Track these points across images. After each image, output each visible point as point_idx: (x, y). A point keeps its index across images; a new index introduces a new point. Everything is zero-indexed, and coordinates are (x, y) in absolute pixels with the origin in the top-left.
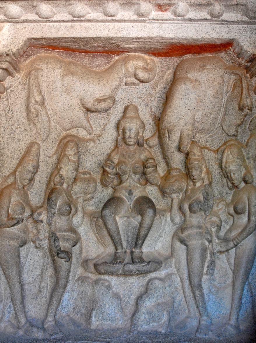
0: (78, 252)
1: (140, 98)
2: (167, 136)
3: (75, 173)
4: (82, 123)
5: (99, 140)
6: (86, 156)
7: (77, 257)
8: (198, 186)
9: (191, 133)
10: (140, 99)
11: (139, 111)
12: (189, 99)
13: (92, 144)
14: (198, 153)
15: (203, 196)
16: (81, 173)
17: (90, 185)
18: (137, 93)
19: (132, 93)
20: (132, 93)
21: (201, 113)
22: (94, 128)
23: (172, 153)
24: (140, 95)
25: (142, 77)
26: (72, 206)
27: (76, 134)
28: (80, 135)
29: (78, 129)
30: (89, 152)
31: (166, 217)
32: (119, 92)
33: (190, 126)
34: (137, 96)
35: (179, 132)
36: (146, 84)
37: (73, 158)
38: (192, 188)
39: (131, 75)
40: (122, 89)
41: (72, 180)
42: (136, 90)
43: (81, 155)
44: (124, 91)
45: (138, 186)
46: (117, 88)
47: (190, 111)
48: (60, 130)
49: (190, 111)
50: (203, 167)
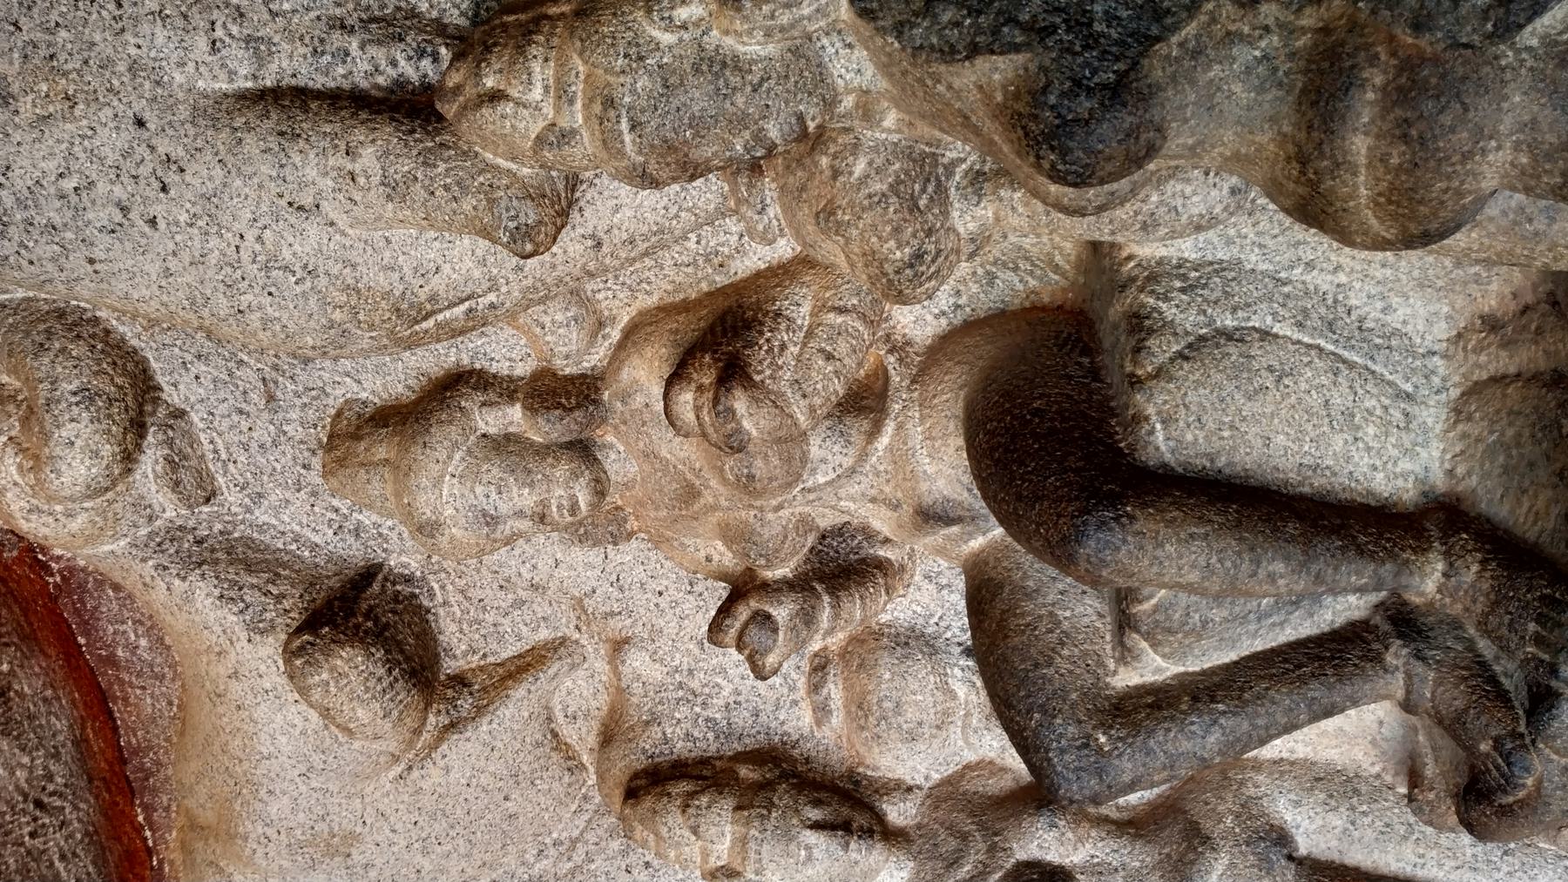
0: (1338, 821)
1: (271, 398)
2: (459, 310)
3: (811, 837)
4: (516, 727)
5: (612, 614)
6: (718, 685)
7: (1370, 834)
8: (870, 70)
9: (368, 158)
10: (279, 394)
11: (364, 395)
12: (69, 184)
13: (637, 662)
14: (537, 93)
15: (974, 51)
16: (819, 723)
17: (887, 704)
18: (241, 412)
19: (254, 445)
20: (254, 445)
21: (161, 35)
22: (544, 634)
23: (599, 245)
24: (254, 396)
25: (96, 454)
26: (1021, 855)
27: (596, 725)
28: (594, 704)
29: (560, 718)
30: (690, 672)
31: (1154, 275)
32: (274, 521)
33: (311, 173)
34: (266, 415)
35: (397, 234)
36: (154, 365)
37: (719, 847)
38: (897, 106)
39: (118, 507)
40: (249, 510)
41: (854, 855)
42: (226, 423)
43: (707, 720)
44: (260, 495)
45: (889, 448)
46: (236, 560)
47: (172, 178)
48: (579, 810)
49: (172, 178)
50: (667, 38)
